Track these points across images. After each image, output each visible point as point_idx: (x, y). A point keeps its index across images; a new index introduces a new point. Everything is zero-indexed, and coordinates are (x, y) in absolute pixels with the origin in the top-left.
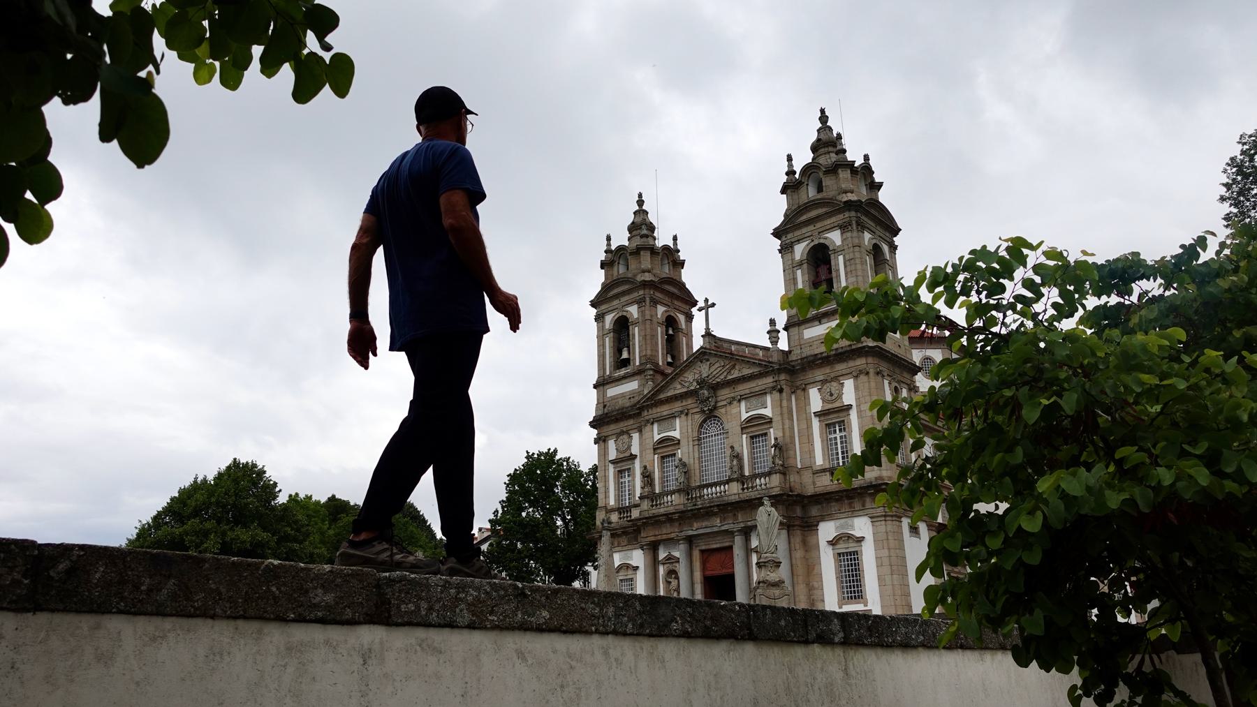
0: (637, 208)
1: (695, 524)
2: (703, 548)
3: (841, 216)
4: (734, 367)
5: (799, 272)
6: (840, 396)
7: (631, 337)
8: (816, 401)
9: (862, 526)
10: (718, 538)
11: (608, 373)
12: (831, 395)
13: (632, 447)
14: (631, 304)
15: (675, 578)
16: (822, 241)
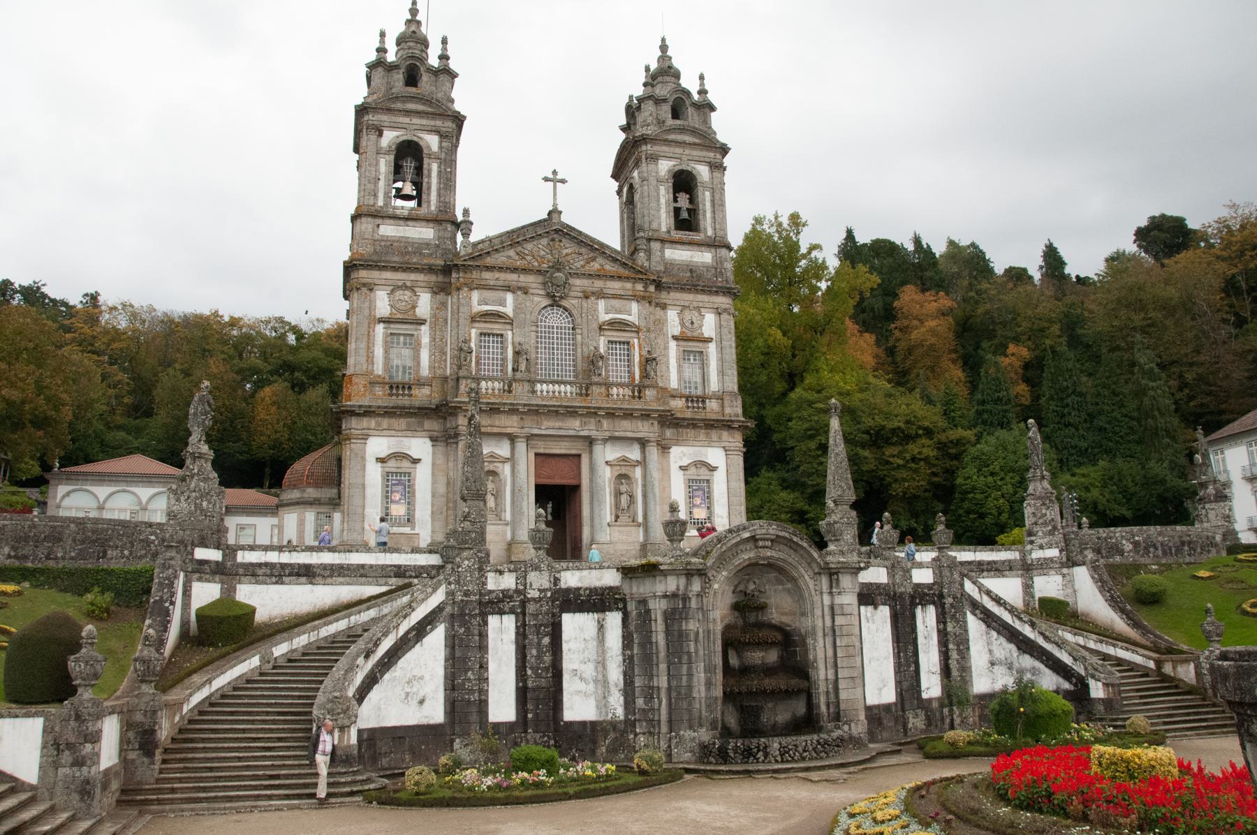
0: (410, 17)
1: (545, 423)
2: (542, 451)
3: (712, 155)
4: (594, 259)
5: (662, 190)
6: (701, 326)
7: (425, 172)
8: (673, 321)
9: (715, 456)
10: (564, 444)
11: (380, 203)
12: (692, 323)
13: (417, 310)
14: (430, 131)
15: (492, 481)
16: (689, 169)
